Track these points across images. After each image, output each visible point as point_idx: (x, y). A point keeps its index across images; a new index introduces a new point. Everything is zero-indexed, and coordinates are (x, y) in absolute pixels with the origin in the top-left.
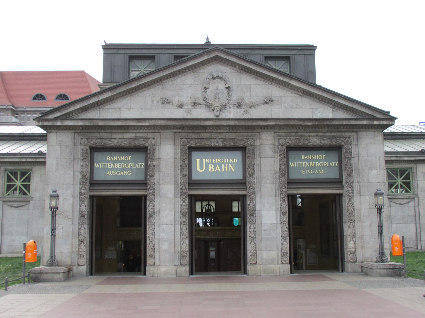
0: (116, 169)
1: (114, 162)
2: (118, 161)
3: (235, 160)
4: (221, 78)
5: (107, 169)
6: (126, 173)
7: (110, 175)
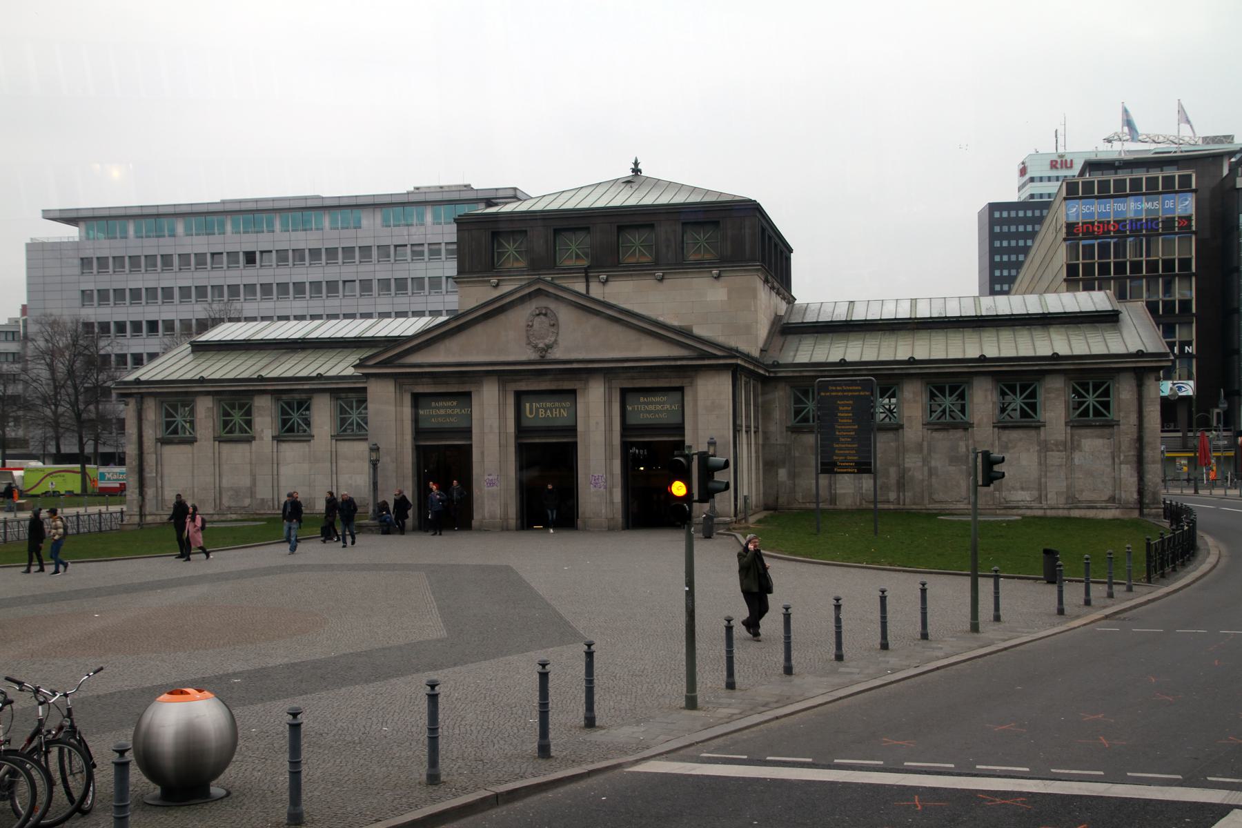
0: (442, 416)
1: (438, 408)
2: (443, 407)
3: (568, 404)
4: (545, 315)
5: (433, 416)
6: (453, 420)
7: (433, 423)
